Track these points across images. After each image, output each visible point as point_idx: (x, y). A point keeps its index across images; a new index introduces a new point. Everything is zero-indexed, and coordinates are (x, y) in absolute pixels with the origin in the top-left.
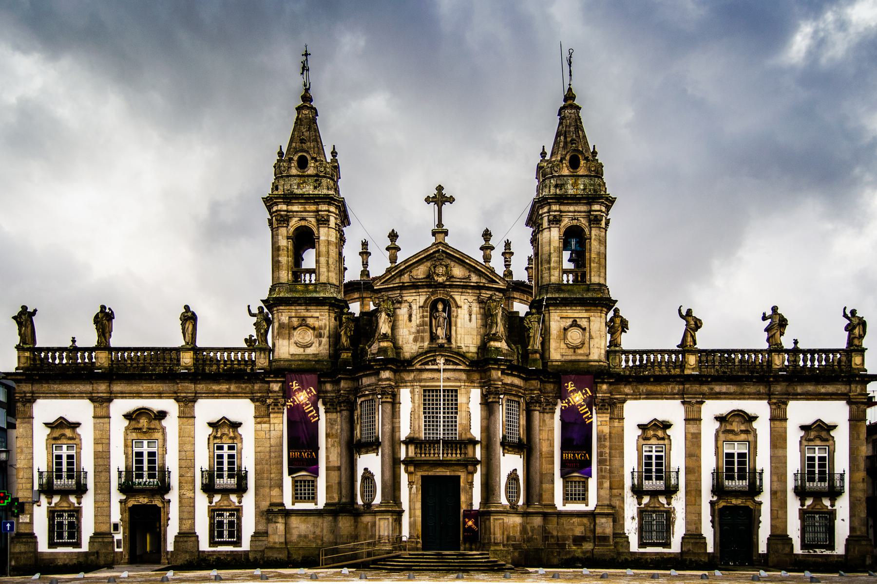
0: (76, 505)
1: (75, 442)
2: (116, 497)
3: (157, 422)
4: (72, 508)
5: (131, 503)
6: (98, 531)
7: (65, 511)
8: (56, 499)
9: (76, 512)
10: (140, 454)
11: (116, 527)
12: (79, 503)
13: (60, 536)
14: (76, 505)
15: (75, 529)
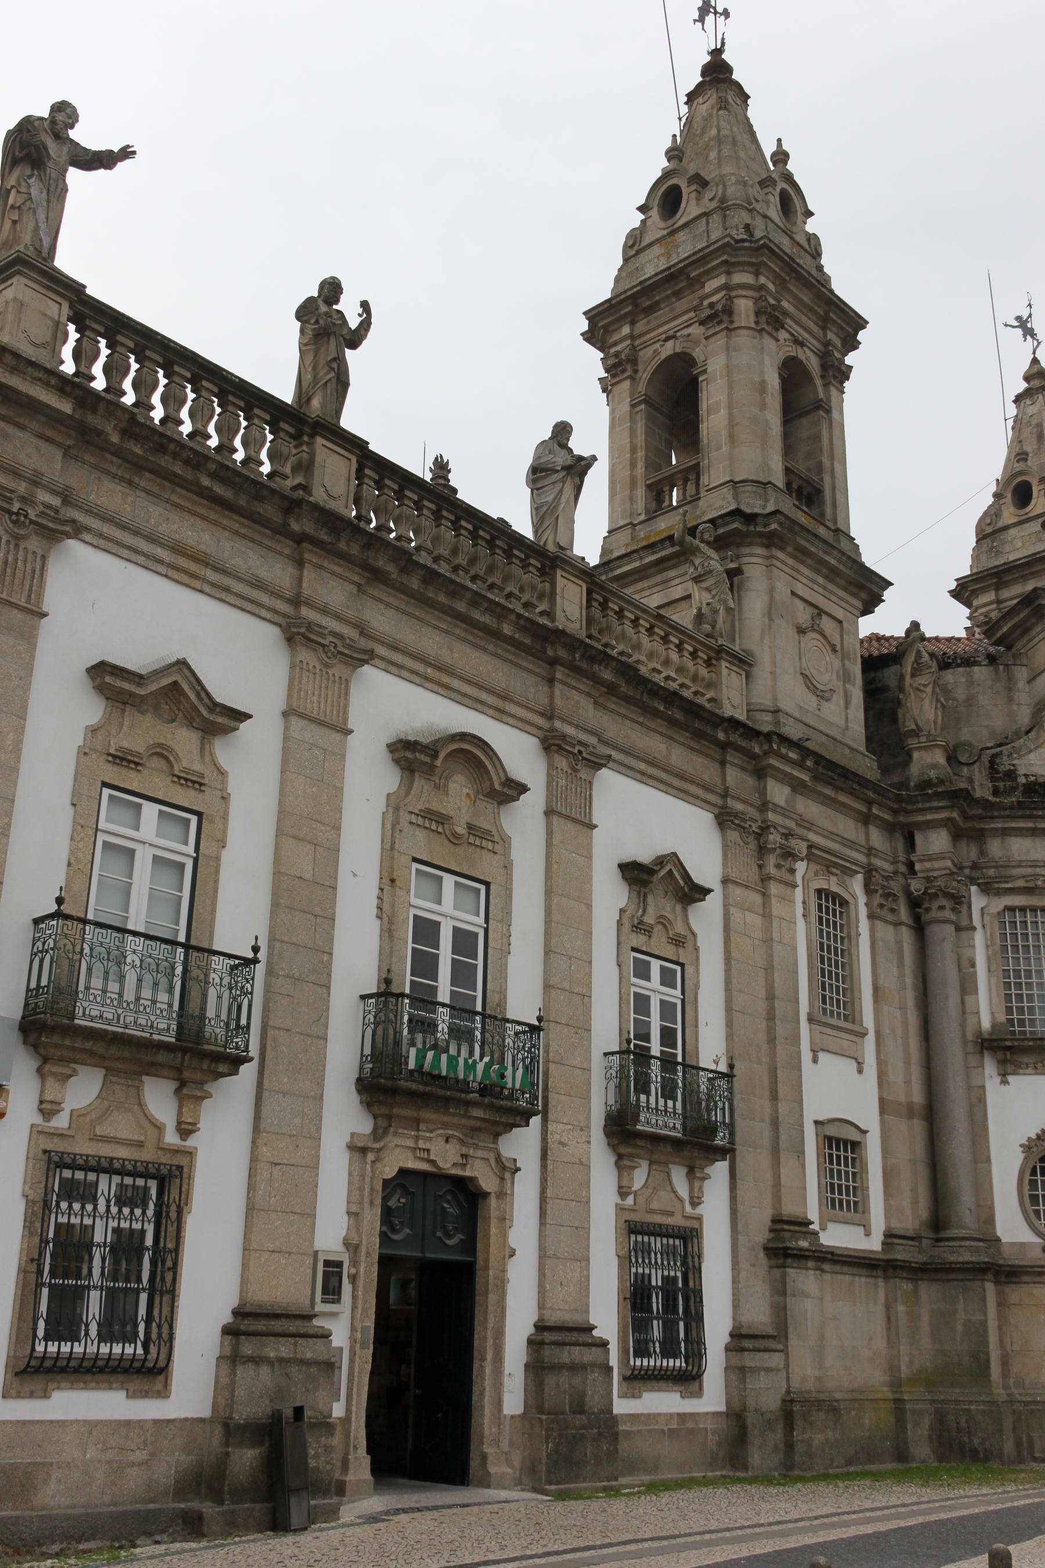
0: (171, 1138)
1: (198, 806)
2: (343, 1116)
3: (491, 807)
4: (147, 1155)
5: (399, 1156)
6: (264, 1295)
7: (108, 1167)
8: (83, 1090)
9: (164, 1184)
10: (426, 931)
11: (332, 1272)
12: (186, 1130)
13: (64, 1323)
14: (171, 1138)
15: (149, 1266)
